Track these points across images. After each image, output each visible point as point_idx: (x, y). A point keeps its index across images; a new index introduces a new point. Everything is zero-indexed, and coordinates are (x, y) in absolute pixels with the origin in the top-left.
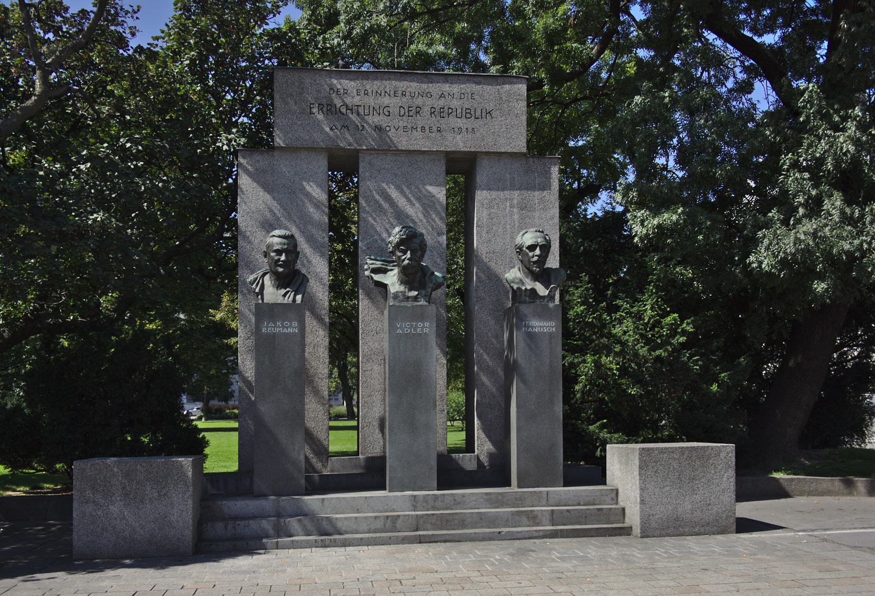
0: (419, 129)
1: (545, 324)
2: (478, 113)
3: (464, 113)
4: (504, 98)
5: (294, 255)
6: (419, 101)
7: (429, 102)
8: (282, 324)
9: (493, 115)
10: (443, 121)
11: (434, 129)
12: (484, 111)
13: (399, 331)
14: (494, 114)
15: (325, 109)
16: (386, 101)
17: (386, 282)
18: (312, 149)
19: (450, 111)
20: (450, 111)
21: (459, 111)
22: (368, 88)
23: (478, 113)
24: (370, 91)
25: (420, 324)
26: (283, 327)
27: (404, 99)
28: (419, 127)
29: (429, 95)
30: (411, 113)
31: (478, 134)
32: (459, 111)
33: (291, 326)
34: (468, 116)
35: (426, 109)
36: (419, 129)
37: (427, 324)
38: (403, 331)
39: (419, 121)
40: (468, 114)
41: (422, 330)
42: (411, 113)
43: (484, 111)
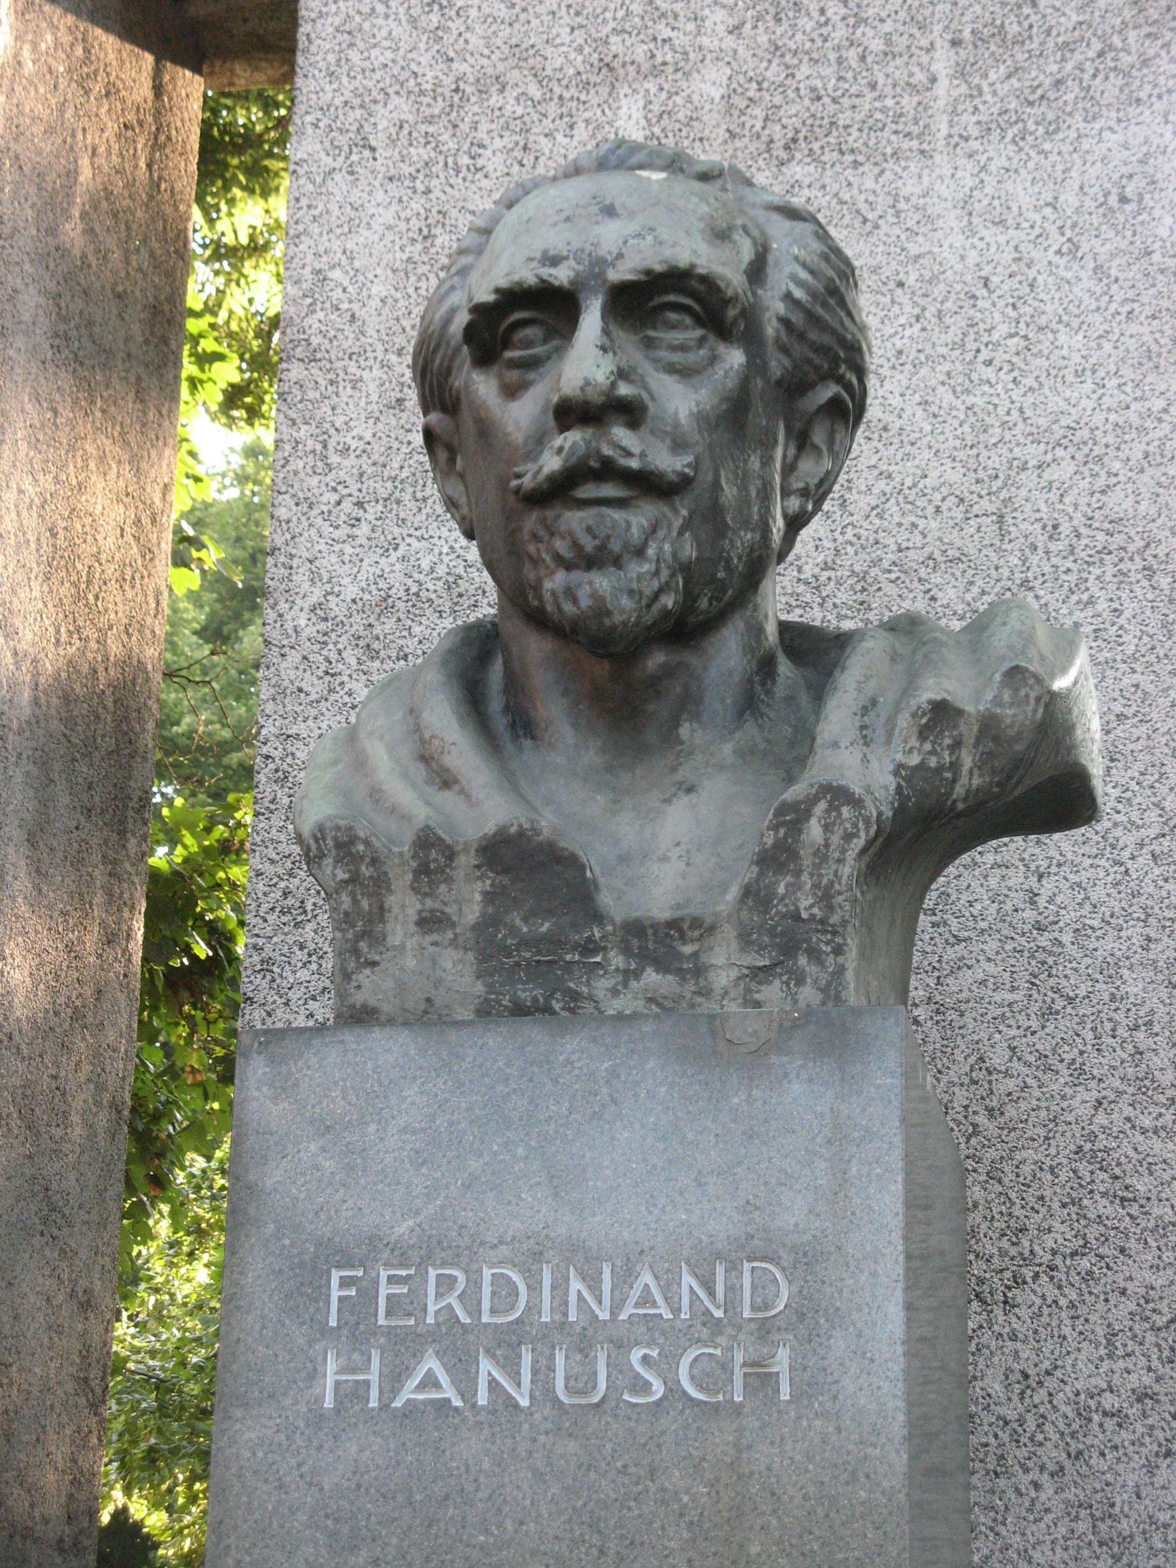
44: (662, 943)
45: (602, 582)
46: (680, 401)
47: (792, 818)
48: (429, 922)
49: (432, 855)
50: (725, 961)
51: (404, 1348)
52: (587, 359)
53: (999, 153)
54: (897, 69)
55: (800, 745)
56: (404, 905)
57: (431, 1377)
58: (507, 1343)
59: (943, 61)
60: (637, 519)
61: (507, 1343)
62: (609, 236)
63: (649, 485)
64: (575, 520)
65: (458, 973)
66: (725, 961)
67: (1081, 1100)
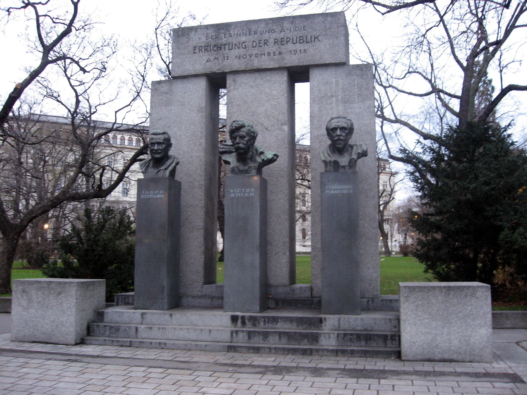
0: (266, 55)
1: (344, 187)
2: (309, 37)
3: (298, 40)
4: (328, 27)
5: (164, 146)
6: (266, 36)
7: (274, 36)
8: (154, 192)
9: (320, 39)
10: (283, 47)
11: (277, 53)
12: (313, 37)
13: (233, 195)
14: (320, 38)
15: (203, 50)
16: (243, 39)
17: (229, 160)
18: (196, 76)
19: (288, 40)
20: (288, 40)
21: (295, 39)
22: (231, 32)
23: (309, 37)
24: (233, 34)
25: (248, 190)
26: (154, 194)
27: (256, 36)
28: (266, 52)
29: (272, 31)
30: (260, 45)
31: (308, 53)
32: (295, 39)
33: (159, 193)
34: (301, 41)
35: (272, 40)
36: (266, 55)
37: (253, 190)
38: (235, 195)
39: (266, 49)
40: (302, 40)
41: (249, 194)
42: (260, 45)
43: (313, 37)
44: (344, 167)
45: (339, 146)
46: (344, 134)
47: (351, 160)
48: (330, 166)
49: (330, 162)
50: (347, 168)
51: (331, 190)
52: (338, 132)
53: (360, 103)
54: (353, 97)
55: (351, 155)
56: (328, 165)
57: (332, 192)
58: (336, 190)
59: (356, 96)
60: (341, 142)
61: (336, 190)
62: (339, 124)
63: (342, 140)
64: (338, 142)
65: (332, 168)
66: (347, 168)
67: (366, 170)
